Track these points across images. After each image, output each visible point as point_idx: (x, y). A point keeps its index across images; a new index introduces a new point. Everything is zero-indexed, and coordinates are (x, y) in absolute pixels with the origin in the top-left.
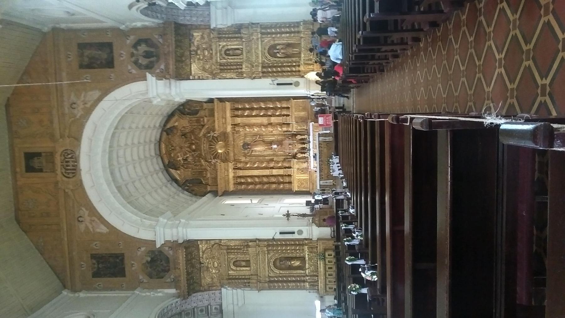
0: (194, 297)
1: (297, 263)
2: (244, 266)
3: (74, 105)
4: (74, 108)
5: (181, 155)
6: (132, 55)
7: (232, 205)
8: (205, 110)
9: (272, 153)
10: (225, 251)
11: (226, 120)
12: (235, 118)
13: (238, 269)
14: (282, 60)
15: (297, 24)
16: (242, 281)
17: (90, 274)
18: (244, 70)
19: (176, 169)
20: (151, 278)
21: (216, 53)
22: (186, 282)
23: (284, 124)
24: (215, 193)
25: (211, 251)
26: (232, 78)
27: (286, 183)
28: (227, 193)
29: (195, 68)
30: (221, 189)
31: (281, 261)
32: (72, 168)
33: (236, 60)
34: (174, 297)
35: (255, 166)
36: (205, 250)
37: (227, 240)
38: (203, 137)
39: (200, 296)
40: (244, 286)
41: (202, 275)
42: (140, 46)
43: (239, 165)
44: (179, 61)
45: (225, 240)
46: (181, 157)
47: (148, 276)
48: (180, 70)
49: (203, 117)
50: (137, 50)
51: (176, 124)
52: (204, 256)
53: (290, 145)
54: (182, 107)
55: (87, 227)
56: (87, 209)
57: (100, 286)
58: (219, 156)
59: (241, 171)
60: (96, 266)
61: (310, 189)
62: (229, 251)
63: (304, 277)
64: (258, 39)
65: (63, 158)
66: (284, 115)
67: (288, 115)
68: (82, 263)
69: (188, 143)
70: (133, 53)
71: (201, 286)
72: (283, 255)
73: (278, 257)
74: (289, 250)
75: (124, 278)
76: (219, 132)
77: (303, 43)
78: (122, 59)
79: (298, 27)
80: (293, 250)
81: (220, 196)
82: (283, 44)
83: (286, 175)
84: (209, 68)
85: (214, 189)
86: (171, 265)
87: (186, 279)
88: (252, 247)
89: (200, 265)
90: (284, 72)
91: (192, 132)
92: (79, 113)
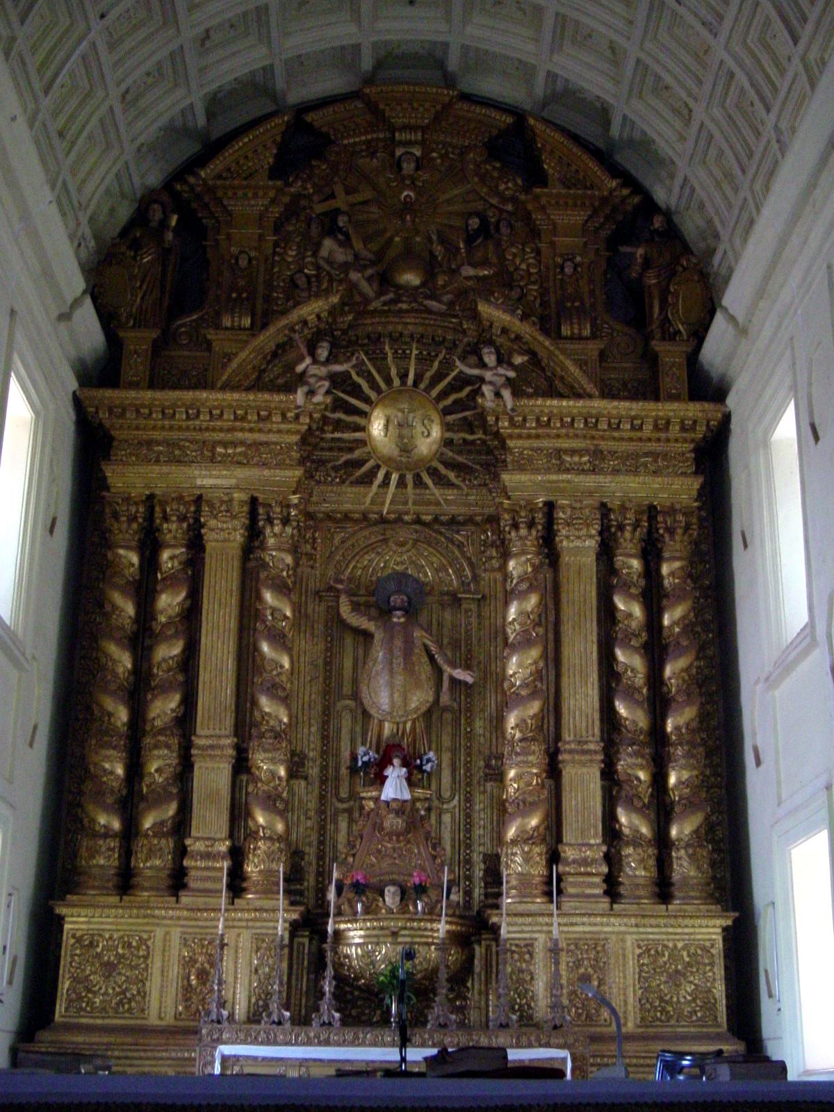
19: (276, 172)
23: (554, 857)
27: (127, 853)
35: (265, 647)
43: (275, 535)
46: (352, 205)
61: (69, 1028)
66: (612, 860)
69: (438, 249)
81: (77, 402)
83: (181, 852)
85: (136, 365)
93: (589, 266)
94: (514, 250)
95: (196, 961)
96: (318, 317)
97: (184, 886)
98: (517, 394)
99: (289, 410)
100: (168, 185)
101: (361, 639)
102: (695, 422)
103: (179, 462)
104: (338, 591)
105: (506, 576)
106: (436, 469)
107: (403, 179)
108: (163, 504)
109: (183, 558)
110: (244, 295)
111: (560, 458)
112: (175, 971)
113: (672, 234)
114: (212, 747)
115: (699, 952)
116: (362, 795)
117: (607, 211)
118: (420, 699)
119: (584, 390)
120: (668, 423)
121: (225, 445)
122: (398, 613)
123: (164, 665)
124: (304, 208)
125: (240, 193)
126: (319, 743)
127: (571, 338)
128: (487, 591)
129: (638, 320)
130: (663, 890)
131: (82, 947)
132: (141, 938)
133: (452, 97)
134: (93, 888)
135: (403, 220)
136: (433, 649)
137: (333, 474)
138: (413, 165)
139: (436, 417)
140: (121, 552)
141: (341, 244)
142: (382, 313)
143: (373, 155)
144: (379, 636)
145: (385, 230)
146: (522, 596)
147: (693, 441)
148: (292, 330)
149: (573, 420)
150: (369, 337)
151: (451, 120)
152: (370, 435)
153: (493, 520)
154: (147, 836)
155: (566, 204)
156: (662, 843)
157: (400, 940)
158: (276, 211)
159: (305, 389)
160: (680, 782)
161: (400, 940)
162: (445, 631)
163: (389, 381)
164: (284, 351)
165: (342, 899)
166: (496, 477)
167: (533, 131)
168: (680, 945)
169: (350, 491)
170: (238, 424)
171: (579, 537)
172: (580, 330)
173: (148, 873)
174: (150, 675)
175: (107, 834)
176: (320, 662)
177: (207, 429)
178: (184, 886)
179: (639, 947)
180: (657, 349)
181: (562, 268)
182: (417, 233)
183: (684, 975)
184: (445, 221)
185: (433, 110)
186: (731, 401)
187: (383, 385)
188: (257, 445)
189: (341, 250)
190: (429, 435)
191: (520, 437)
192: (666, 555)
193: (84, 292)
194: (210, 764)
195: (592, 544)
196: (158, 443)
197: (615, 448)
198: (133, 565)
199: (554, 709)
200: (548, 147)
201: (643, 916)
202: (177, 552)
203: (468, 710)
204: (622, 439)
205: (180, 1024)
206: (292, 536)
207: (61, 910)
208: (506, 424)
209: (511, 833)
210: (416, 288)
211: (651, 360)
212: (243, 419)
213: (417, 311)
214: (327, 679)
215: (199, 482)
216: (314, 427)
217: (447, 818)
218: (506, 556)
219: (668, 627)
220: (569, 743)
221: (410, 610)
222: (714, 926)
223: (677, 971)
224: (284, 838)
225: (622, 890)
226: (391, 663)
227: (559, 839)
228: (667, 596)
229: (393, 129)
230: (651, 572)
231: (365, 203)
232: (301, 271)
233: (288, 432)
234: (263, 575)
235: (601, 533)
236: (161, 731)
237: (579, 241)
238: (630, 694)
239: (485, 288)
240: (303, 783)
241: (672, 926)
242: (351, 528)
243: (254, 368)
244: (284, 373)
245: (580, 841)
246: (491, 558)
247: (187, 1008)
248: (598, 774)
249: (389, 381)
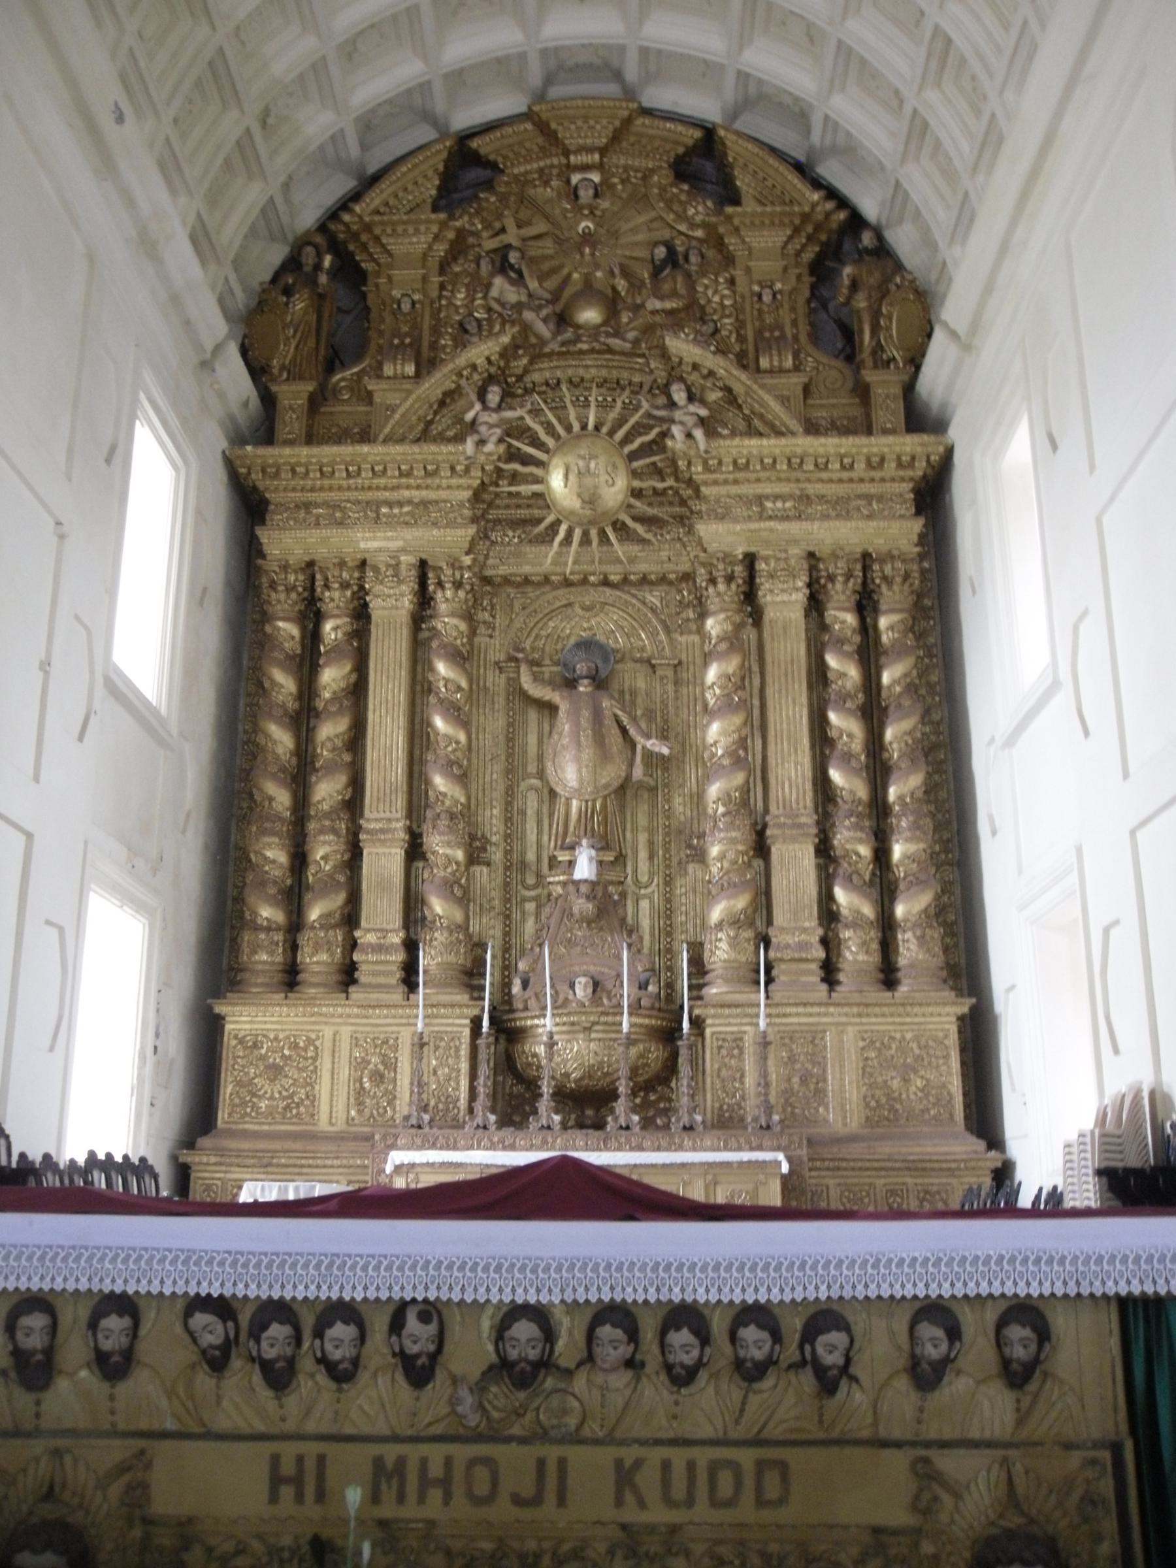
9: (531, 856)
27: (293, 947)
35: (439, 723)
43: (446, 601)
46: (524, 240)
49: (797, 368)
53: (596, 984)
58: (527, 460)
67: (829, 972)
69: (621, 284)
83: (353, 945)
93: (791, 293)
94: (706, 281)
95: (369, 1062)
96: (488, 359)
97: (354, 981)
98: (710, 433)
99: (458, 463)
100: (322, 228)
101: (546, 712)
102: (913, 458)
103: (340, 524)
104: (516, 660)
106: (624, 524)
107: (582, 208)
109: (348, 629)
110: (408, 341)
111: (761, 505)
112: (344, 1073)
114: (382, 831)
115: (931, 1043)
116: (551, 879)
117: (810, 229)
119: (787, 427)
120: (883, 459)
121: (390, 505)
122: (586, 681)
123: (329, 745)
124: (473, 246)
125: (400, 229)
126: (502, 827)
127: (771, 372)
128: (684, 657)
129: (849, 354)
130: (888, 976)
131: (245, 1048)
132: (308, 1038)
133: (632, 111)
134: (256, 985)
135: (582, 254)
136: (625, 720)
137: (511, 534)
138: (591, 192)
139: (621, 465)
140: (281, 624)
141: (512, 282)
142: (561, 354)
143: (546, 183)
144: (564, 707)
145: (562, 266)
147: (911, 479)
148: (460, 375)
149: (775, 461)
150: (547, 384)
151: (632, 139)
152: (548, 487)
153: (687, 577)
154: (313, 928)
155: (763, 223)
157: (593, 1035)
158: (441, 249)
159: (476, 437)
160: (905, 856)
161: (593, 1035)
162: (639, 700)
164: (453, 400)
165: (530, 992)
166: (690, 531)
167: (723, 144)
168: (909, 1036)
169: (531, 551)
170: (404, 480)
171: (783, 591)
172: (780, 361)
173: (316, 968)
174: (315, 756)
176: (501, 738)
177: (370, 488)
178: (354, 981)
179: (863, 1039)
180: (868, 379)
181: (760, 296)
182: (597, 266)
183: (915, 1071)
184: (627, 253)
185: (611, 128)
186: (954, 433)
187: (560, 429)
188: (425, 503)
189: (513, 289)
190: (613, 484)
191: (715, 483)
192: (883, 607)
193: (228, 337)
194: (380, 850)
195: (800, 597)
196: (317, 506)
197: (823, 492)
198: (293, 638)
200: (741, 161)
201: (867, 1005)
202: (339, 622)
203: (666, 785)
204: (831, 481)
205: (353, 1129)
206: (466, 601)
208: (700, 469)
209: (716, 913)
210: (597, 327)
211: (863, 392)
212: (409, 474)
213: (599, 352)
214: (510, 756)
215: (362, 545)
216: (486, 480)
217: (644, 904)
218: (703, 616)
219: (889, 687)
220: (777, 817)
221: (600, 683)
222: (948, 1015)
223: (905, 1065)
224: (464, 927)
225: (841, 977)
226: (579, 736)
227: (769, 922)
228: (885, 653)
229: (566, 153)
230: (867, 629)
231: (538, 237)
232: (471, 314)
233: (459, 487)
235: (809, 585)
236: (327, 815)
237: (780, 264)
239: (675, 321)
240: (485, 869)
241: (900, 1015)
242: (531, 592)
243: (419, 419)
244: (454, 424)
245: (793, 925)
246: (688, 620)
247: (360, 1112)
248: (812, 850)
249: (569, 428)
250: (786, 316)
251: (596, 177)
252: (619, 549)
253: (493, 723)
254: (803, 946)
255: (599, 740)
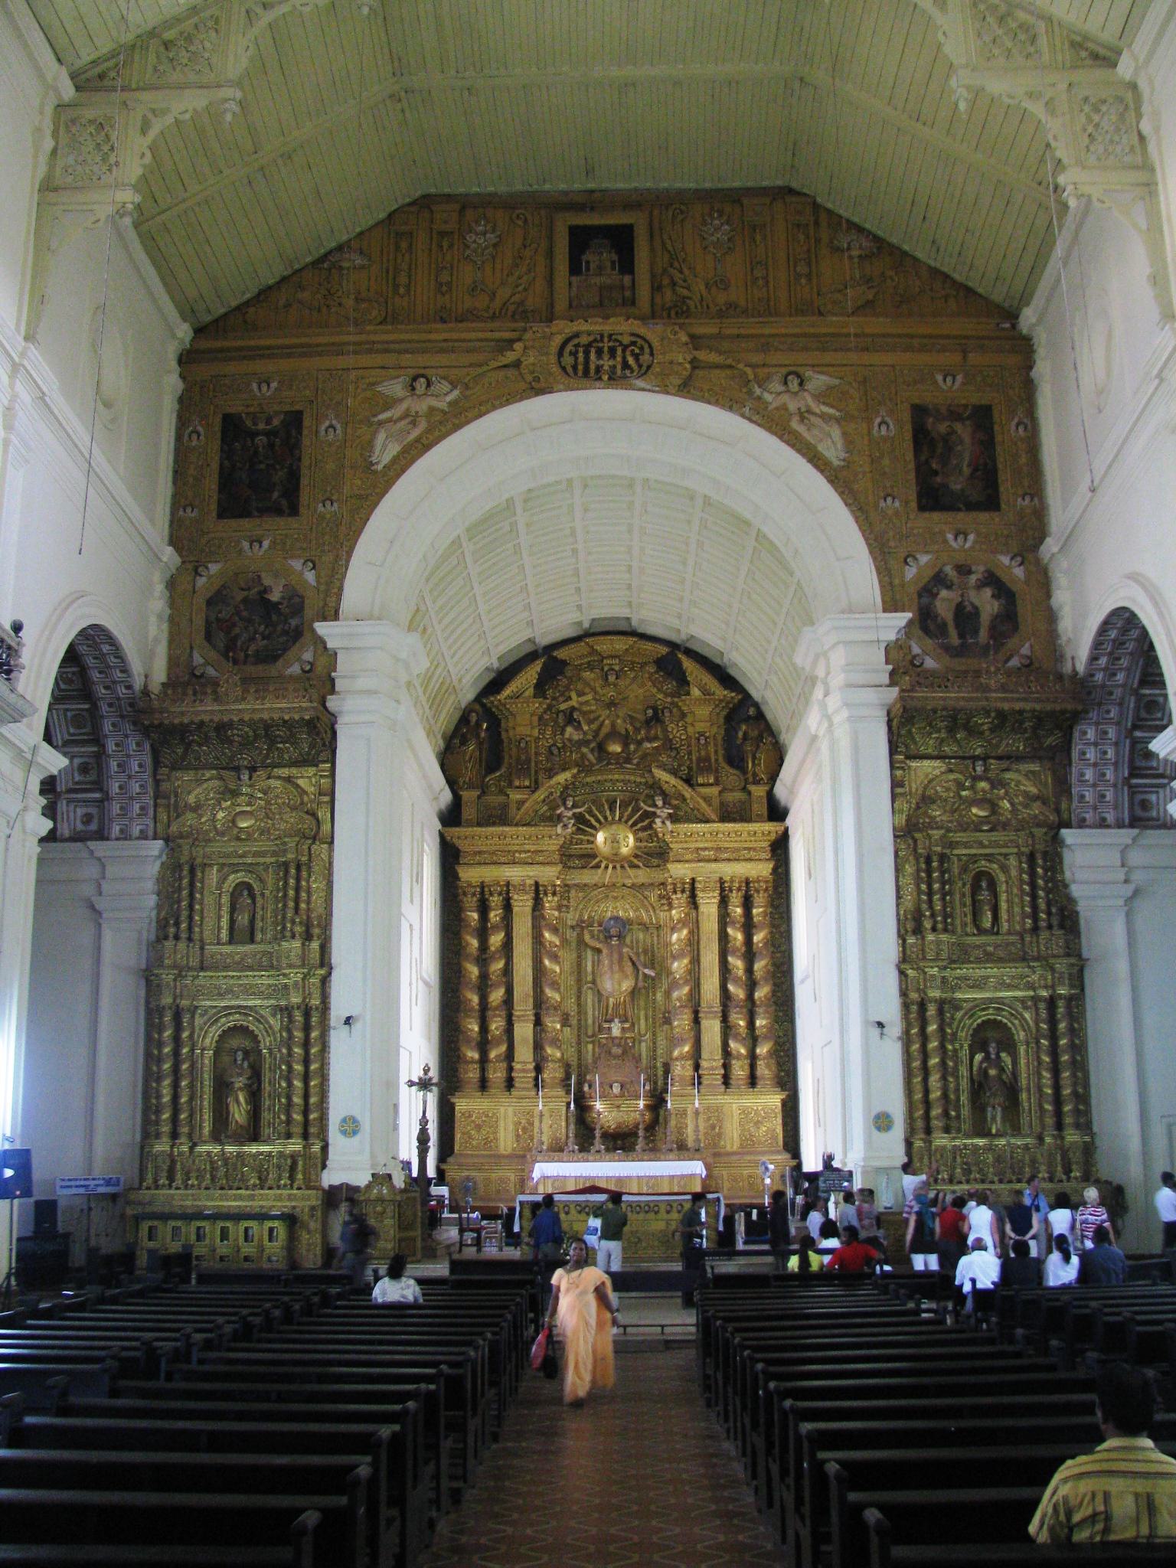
0: (138, 744)
1: (239, 1112)
2: (232, 922)
3: (796, 382)
4: (786, 383)
5: (587, 703)
6: (964, 570)
7: (418, 878)
8: (744, 789)
9: (590, 1021)
10: (290, 856)
11: (709, 861)
12: (717, 893)
13: (225, 900)
14: (964, 1071)
15: (1084, 1124)
16: (185, 914)
17: (236, 407)
18: (930, 937)
19: (540, 688)
20: (209, 602)
21: (981, 845)
22: (197, 719)
24: (451, 817)
25: (293, 808)
26: (899, 897)
27: (483, 1070)
28: (450, 857)
29: (926, 769)
30: (471, 837)
31: (247, 1054)
32: (592, 367)
33: (962, 914)
34: (146, 676)
35: (547, 962)
36: (298, 786)
37: (331, 864)
38: (650, 781)
39: (140, 765)
40: (166, 919)
41: (208, 774)
42: (993, 596)
43: (549, 902)
44: (954, 718)
45: (331, 857)
46: (581, 704)
47: (218, 592)
48: (923, 725)
50: (981, 585)
51: (696, 692)
52: (277, 783)
54: (752, 711)
55: (389, 403)
56: (450, 403)
57: (194, 436)
59: (528, 910)
60: (261, 426)
62: (293, 871)
63: (190, 1136)
64: (1031, 986)
65: (626, 340)
67: (726, 1080)
68: (274, 385)
70: (970, 572)
71: (173, 768)
72: (268, 1060)
73: (262, 1045)
74: (290, 1084)
75: (214, 514)
76: (668, 838)
77: (1019, 1142)
78: (950, 537)
79: (1077, 1126)
80: (289, 1098)
81: (442, 835)
82: (1015, 1075)
83: (510, 1069)
84: (932, 818)
85: (468, 812)
86: (252, 670)
87: (206, 718)
88: (303, 950)
89: (247, 768)
90: (925, 1080)
91: (669, 745)
92: (772, 395)
100: (478, 699)
105: (671, 918)
108: (489, 886)
112: (511, 1127)
113: (760, 716)
118: (627, 985)
144: (605, 951)
146: (680, 930)
156: (753, 1057)
163: (606, 818)
175: (473, 1061)
199: (696, 986)
207: (453, 1100)
209: (676, 1053)
214: (579, 973)
217: (643, 1044)
224: (561, 1060)
234: (543, 923)
236: (496, 1008)
238: (736, 980)
250: (711, 749)
251: (617, 668)
252: (631, 872)
253: (568, 957)
254: (712, 1068)
255: (621, 969)
